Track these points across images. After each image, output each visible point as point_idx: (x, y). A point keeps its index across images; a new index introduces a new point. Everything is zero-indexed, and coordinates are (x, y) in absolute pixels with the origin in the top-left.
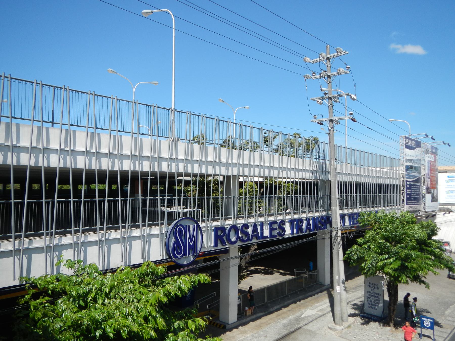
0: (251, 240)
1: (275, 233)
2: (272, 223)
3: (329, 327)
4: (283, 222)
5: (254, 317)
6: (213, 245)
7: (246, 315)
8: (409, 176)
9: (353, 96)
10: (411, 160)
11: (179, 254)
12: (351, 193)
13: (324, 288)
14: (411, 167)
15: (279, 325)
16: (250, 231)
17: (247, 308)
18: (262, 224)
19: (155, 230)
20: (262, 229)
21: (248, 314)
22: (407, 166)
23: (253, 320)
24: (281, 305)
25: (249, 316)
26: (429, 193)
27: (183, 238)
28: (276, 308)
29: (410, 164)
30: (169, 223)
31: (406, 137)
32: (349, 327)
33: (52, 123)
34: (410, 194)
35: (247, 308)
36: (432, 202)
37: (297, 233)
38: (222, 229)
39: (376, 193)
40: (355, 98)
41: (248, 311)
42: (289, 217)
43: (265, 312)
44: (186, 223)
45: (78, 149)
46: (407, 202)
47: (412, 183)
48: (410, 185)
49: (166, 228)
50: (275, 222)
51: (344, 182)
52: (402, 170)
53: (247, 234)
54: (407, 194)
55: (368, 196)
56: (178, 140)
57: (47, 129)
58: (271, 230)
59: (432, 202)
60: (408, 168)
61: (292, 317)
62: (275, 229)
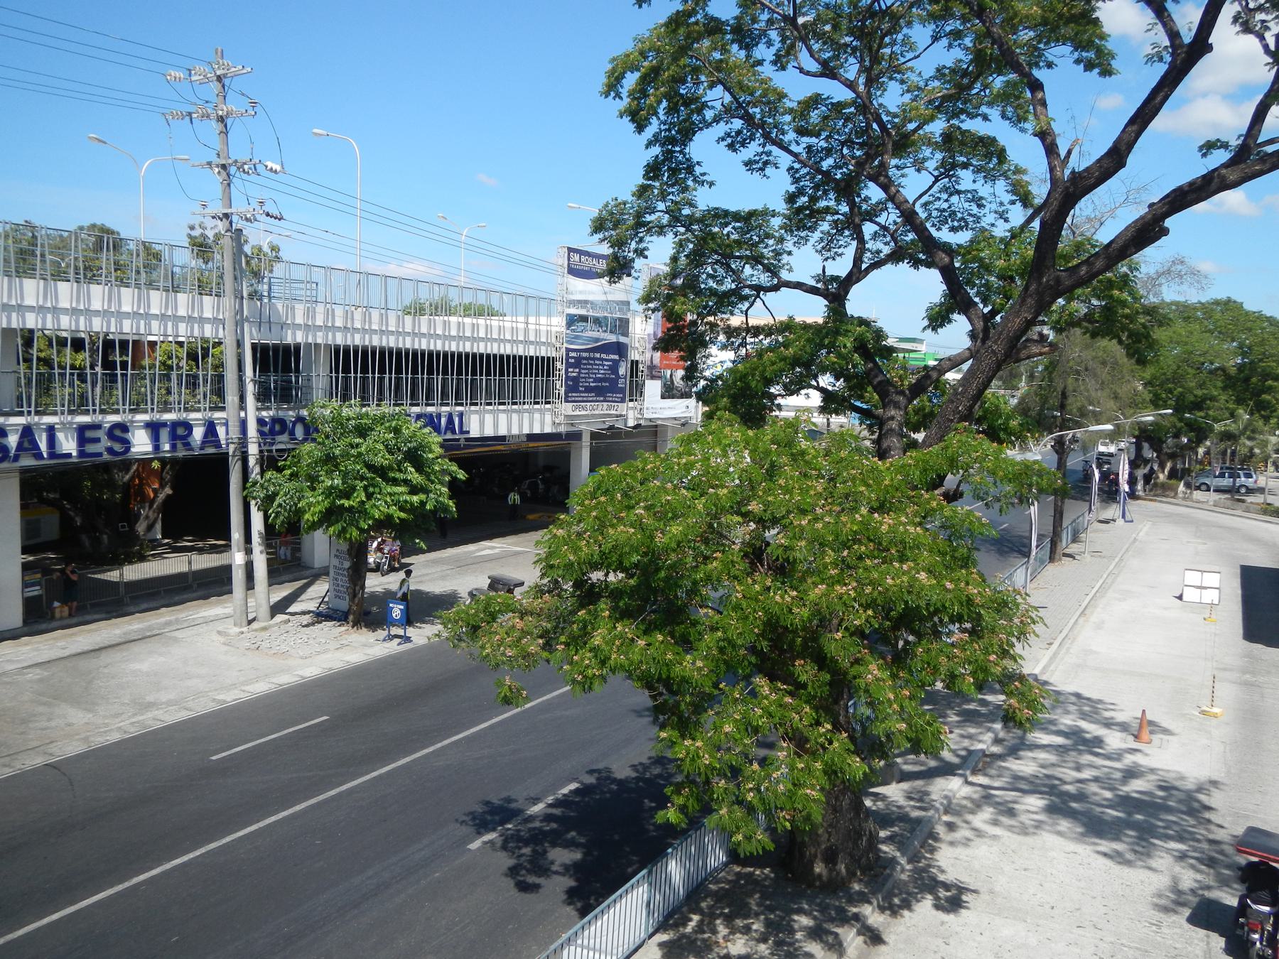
0: (16, 458)
1: (91, 448)
2: (82, 429)
3: (219, 633)
4: (123, 427)
5: (75, 620)
7: (53, 618)
9: (270, 164)
10: (584, 303)
13: (308, 572)
14: (584, 319)
15: (117, 632)
17: (56, 604)
18: (51, 430)
21: (57, 615)
23: (63, 628)
24: (163, 602)
25: (61, 618)
26: (653, 377)
28: (144, 606)
29: (583, 312)
31: (570, 250)
32: (265, 629)
34: (576, 380)
36: (663, 397)
37: (174, 447)
39: (459, 373)
40: (278, 168)
41: (57, 611)
42: (143, 417)
43: (108, 612)
46: (566, 396)
47: (585, 355)
50: (96, 427)
51: (356, 352)
52: (558, 324)
54: (567, 378)
55: (381, 380)
58: (82, 441)
59: (663, 397)
60: (572, 321)
61: (163, 620)
62: (97, 440)
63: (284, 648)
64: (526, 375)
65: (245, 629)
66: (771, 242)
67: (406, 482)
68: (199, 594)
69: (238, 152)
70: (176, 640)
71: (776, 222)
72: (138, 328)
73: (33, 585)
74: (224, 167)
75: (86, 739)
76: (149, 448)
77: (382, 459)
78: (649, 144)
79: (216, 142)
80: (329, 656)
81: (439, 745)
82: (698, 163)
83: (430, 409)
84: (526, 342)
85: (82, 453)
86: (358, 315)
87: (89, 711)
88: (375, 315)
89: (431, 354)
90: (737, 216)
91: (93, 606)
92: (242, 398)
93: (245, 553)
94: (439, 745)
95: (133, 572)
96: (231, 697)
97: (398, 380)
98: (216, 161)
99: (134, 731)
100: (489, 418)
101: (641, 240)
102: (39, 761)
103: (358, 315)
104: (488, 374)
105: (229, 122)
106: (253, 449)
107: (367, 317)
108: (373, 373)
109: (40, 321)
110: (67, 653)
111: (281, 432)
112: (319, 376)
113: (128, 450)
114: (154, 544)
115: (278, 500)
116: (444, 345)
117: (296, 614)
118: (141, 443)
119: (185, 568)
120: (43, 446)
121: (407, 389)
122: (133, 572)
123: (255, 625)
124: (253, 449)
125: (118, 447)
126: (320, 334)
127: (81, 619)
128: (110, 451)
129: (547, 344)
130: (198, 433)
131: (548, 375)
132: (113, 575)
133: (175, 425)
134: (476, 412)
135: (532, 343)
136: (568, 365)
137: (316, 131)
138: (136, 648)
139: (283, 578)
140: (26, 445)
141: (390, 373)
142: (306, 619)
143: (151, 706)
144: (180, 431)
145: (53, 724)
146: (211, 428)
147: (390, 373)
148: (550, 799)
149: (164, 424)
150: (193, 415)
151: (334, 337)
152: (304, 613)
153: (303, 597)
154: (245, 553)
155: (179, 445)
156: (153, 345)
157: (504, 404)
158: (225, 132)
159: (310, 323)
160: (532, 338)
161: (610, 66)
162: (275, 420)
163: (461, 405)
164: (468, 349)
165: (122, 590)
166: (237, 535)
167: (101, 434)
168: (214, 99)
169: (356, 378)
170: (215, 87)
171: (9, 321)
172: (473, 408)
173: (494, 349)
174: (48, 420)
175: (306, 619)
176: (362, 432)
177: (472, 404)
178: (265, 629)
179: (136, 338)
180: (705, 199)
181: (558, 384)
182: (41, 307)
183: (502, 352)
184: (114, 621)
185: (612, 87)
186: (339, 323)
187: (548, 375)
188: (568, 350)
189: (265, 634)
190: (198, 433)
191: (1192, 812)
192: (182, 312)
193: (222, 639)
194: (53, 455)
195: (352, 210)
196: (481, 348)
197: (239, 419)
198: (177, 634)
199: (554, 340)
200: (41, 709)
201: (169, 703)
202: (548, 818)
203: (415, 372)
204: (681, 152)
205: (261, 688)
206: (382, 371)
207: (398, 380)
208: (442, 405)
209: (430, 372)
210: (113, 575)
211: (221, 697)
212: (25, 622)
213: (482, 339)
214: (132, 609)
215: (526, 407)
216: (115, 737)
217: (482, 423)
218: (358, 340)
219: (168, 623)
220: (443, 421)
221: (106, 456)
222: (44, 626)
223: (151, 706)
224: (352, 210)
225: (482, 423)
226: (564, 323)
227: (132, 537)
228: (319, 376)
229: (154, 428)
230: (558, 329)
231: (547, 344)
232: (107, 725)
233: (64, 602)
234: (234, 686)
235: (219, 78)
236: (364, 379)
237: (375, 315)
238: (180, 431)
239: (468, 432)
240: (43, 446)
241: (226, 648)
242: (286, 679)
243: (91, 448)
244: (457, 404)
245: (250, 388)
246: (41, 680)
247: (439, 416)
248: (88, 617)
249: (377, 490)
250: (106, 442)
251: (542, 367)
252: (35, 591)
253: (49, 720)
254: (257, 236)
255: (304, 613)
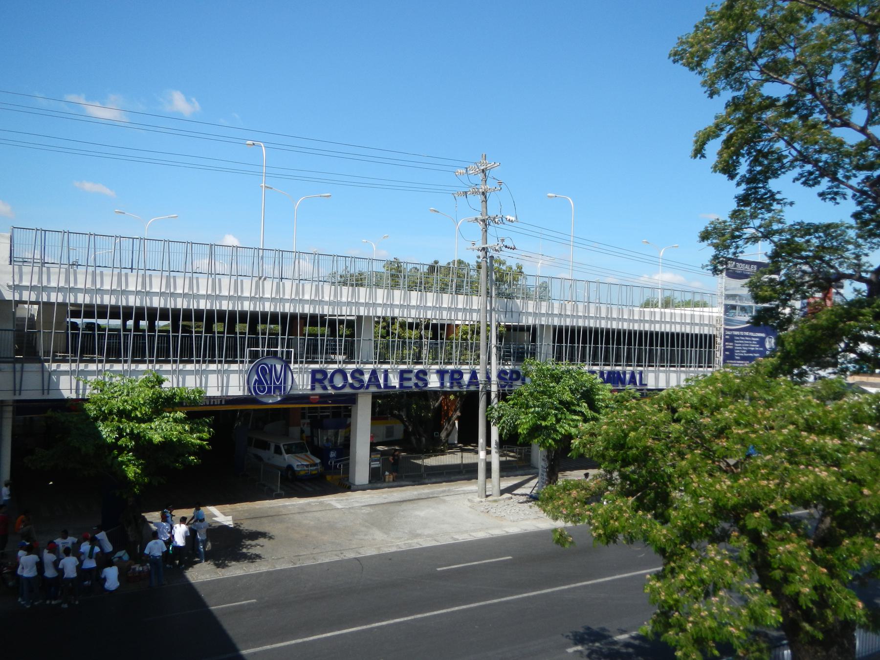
0: (367, 387)
1: (406, 384)
2: (402, 372)
4: (424, 372)
5: (396, 484)
6: (309, 387)
7: (385, 481)
8: (727, 322)
9: (508, 217)
11: (262, 392)
12: (572, 342)
13: (534, 471)
15: (415, 493)
16: (366, 377)
17: (387, 473)
18: (386, 372)
19: (234, 367)
20: (386, 378)
22: (726, 306)
25: (389, 482)
27: (268, 377)
28: (434, 480)
30: (250, 362)
32: (495, 501)
33: (132, 269)
35: (387, 473)
37: (451, 387)
38: (323, 372)
40: (513, 219)
43: (414, 481)
44: (270, 362)
45: (154, 290)
48: (732, 336)
49: (247, 366)
50: (410, 371)
52: (718, 312)
53: (362, 381)
54: (725, 350)
56: (265, 279)
57: (126, 275)
58: (402, 379)
60: (729, 308)
61: (441, 489)
62: (410, 379)
63: (503, 514)
64: (692, 347)
65: (483, 500)
66: (851, 247)
67: (582, 414)
68: (466, 476)
69: (492, 213)
70: (444, 501)
71: (852, 233)
72: (451, 316)
73: (376, 461)
74: (484, 221)
75: (379, 548)
76: (438, 385)
77: (567, 397)
78: (738, 184)
79: (479, 206)
80: (527, 522)
81: (573, 586)
82: (779, 192)
83: (618, 368)
84: (692, 324)
85: (401, 385)
86: (569, 306)
87: (386, 534)
88: (581, 306)
89: (619, 332)
90: (817, 228)
91: (407, 477)
92: (489, 358)
93: (487, 455)
94: (573, 586)
95: (432, 461)
96: (462, 538)
97: (596, 349)
98: (480, 217)
99: (404, 548)
100: (662, 376)
101: (737, 247)
102: (352, 555)
103: (569, 306)
104: (662, 345)
105: (488, 195)
106: (494, 388)
107: (575, 308)
108: (578, 343)
109: (331, 310)
110: (386, 501)
111: (517, 379)
112: (546, 345)
113: (426, 385)
114: (451, 446)
115: (504, 419)
116: (661, 327)
117: (515, 495)
118: (434, 382)
119: (459, 462)
120: (382, 381)
121: (601, 354)
122: (432, 461)
123: (490, 498)
124: (494, 388)
125: (420, 384)
126: (543, 319)
127: (399, 483)
128: (416, 385)
129: (709, 325)
130: (466, 378)
131: (710, 347)
132: (419, 462)
133: (453, 372)
134: (652, 371)
135: (697, 324)
136: (726, 340)
137: (550, 194)
138: (422, 503)
139: (518, 473)
140: (373, 380)
141: (590, 343)
142: (524, 499)
143: (417, 536)
144: (456, 376)
145: (366, 538)
146: (474, 374)
147: (590, 343)
148: (634, 633)
149: (447, 372)
150: (464, 367)
151: (577, 321)
152: (522, 495)
153: (526, 485)
154: (487, 455)
155: (455, 384)
156: (457, 326)
157: (674, 366)
158: (485, 201)
159: (530, 313)
160: (697, 321)
161: (695, 139)
162: (512, 372)
163: (641, 366)
164: (668, 330)
165: (423, 469)
166: (481, 440)
167: (412, 376)
168: (480, 183)
169: (566, 347)
170: (481, 176)
171: (315, 309)
172: (650, 368)
173: (667, 328)
174: (385, 366)
175: (524, 499)
176: (557, 379)
177: (649, 366)
178: (495, 501)
179: (449, 322)
180: (791, 217)
181: (718, 354)
182: (385, 304)
183: (673, 330)
184: (416, 487)
185: (699, 152)
186: (556, 312)
187: (710, 347)
188: (725, 329)
189: (495, 504)
190: (466, 378)
191: (156, 403)
192: (460, 306)
193: (469, 504)
194: (386, 386)
195: (576, 240)
196: (657, 328)
197: (489, 368)
198: (446, 498)
199: (715, 323)
200: (363, 529)
201: (428, 536)
202: (627, 645)
203: (607, 343)
204: (763, 187)
205: (481, 535)
206: (584, 342)
207: (596, 349)
208: (627, 366)
209: (619, 343)
210: (419, 462)
211: (456, 537)
212: (370, 482)
213: (658, 322)
214: (427, 481)
215: (692, 369)
216: (394, 549)
217: (657, 379)
218: (568, 322)
219: (444, 492)
220: (628, 376)
221: (415, 389)
222: (379, 485)
223: (417, 536)
224: (576, 240)
225: (657, 379)
226: (723, 310)
227: (438, 441)
228: (546, 345)
229: (441, 373)
230: (717, 315)
231: (709, 325)
232: (392, 542)
233: (391, 473)
234: (466, 531)
235: (483, 171)
236: (572, 348)
237: (581, 306)
238: (456, 376)
239: (646, 385)
240: (382, 381)
241: (469, 509)
242: (497, 532)
243: (406, 384)
244: (638, 366)
245: (494, 350)
246: (368, 514)
247: (624, 373)
248: (403, 483)
249: (563, 416)
250: (414, 380)
251: (707, 341)
252: (376, 465)
253: (365, 535)
254: (510, 260)
255: (522, 495)
